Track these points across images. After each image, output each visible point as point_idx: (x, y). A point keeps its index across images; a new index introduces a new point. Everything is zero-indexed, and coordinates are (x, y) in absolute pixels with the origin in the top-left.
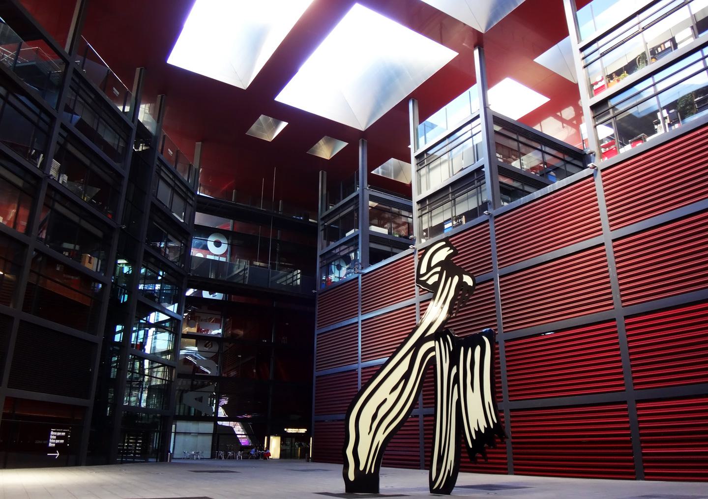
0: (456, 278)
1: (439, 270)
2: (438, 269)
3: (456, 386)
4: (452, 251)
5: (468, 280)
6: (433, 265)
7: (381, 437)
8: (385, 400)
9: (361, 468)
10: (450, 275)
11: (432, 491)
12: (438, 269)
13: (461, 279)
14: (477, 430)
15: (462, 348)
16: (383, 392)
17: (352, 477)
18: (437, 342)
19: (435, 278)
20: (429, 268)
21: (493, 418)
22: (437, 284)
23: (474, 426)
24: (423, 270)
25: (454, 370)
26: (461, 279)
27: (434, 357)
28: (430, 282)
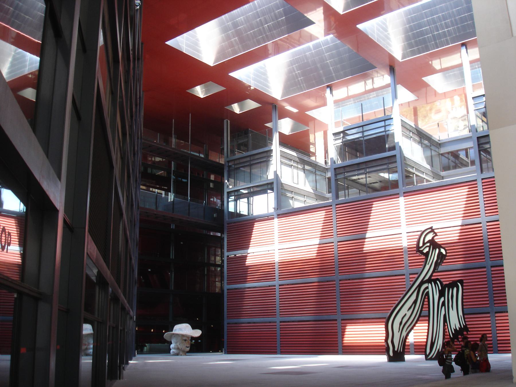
0: (437, 250)
2: (428, 244)
3: (443, 307)
5: (443, 251)
6: (426, 241)
9: (396, 350)
10: (434, 248)
11: (427, 359)
12: (428, 244)
13: (440, 250)
17: (391, 354)
18: (430, 284)
19: (427, 250)
20: (424, 244)
21: (463, 323)
22: (428, 253)
23: (453, 327)
24: (421, 245)
25: (442, 299)
26: (440, 250)
27: (428, 292)
28: (425, 251)
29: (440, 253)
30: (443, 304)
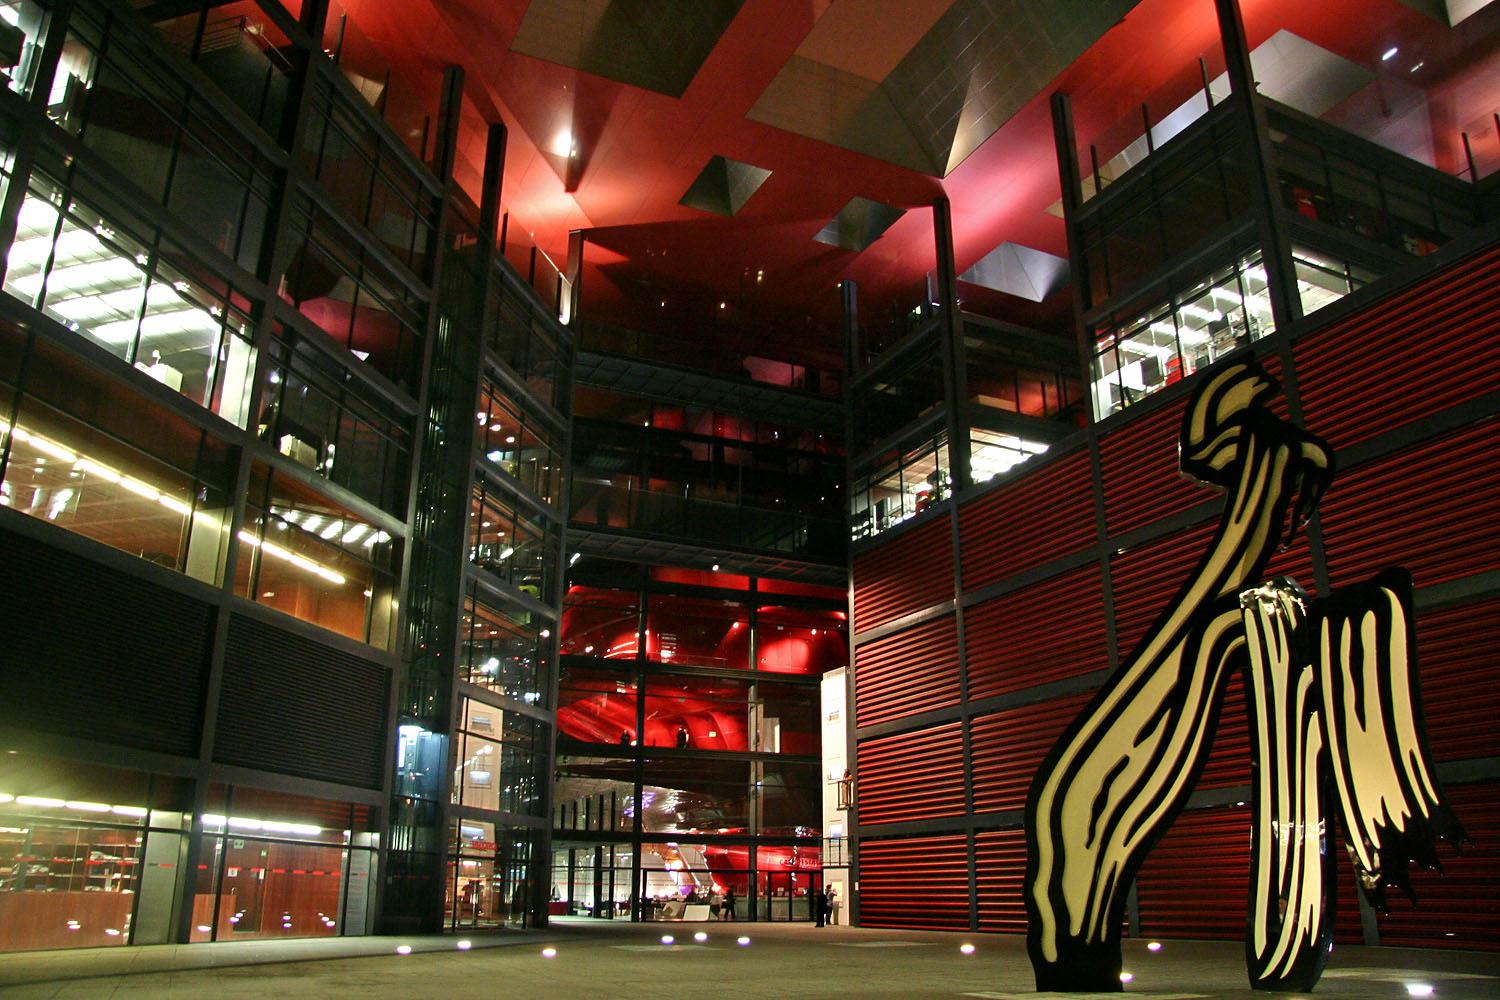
0: (1284, 452)
1: (1237, 434)
2: (1235, 430)
3: (1315, 715)
4: (1265, 385)
5: (1314, 452)
7: (1119, 854)
8: (1124, 762)
9: (1075, 930)
11: (1257, 984)
12: (1235, 430)
14: (1382, 823)
15: (1325, 622)
16: (1119, 740)
17: (1051, 953)
19: (1230, 452)
20: (1212, 428)
22: (1234, 469)
23: (1371, 814)
24: (1197, 432)
25: (1307, 676)
27: (1244, 649)
28: (1218, 462)
29: (1298, 462)
30: (1314, 700)
